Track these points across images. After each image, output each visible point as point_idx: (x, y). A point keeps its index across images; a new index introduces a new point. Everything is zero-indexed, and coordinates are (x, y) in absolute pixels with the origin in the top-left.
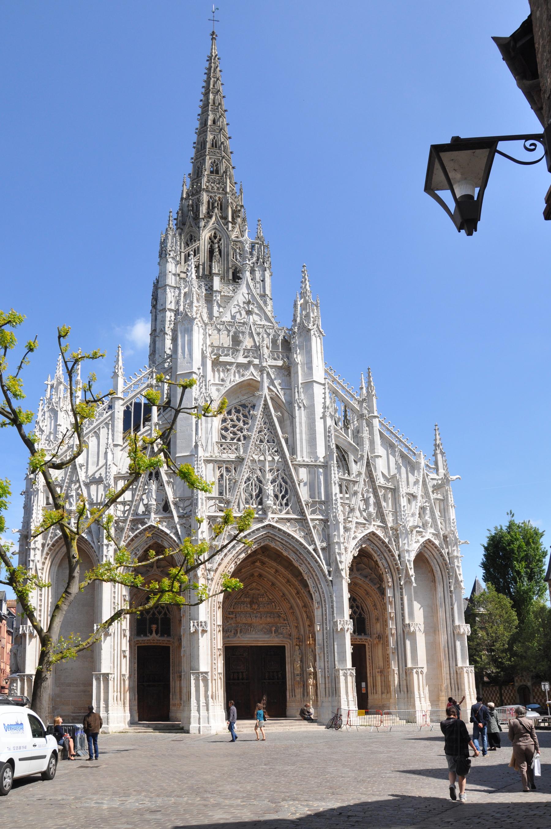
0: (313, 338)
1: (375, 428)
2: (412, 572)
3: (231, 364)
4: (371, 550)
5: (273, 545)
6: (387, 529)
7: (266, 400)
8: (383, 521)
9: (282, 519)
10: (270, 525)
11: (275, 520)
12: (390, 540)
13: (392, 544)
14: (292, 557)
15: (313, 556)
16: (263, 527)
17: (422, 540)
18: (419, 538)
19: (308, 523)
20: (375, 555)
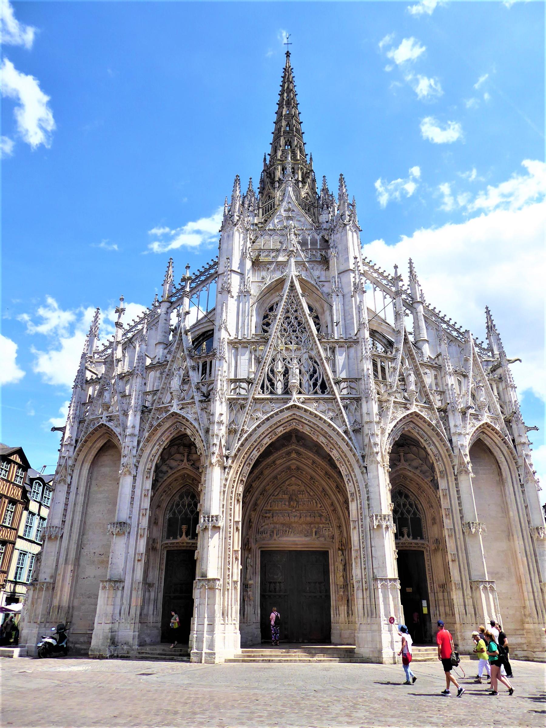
0: (350, 233)
1: (419, 314)
2: (468, 459)
3: (271, 263)
4: (416, 434)
5: (300, 428)
6: (433, 410)
7: (292, 282)
8: (428, 402)
9: (309, 399)
10: (295, 406)
11: (301, 400)
12: (438, 422)
13: (440, 427)
14: (321, 440)
15: (343, 439)
16: (288, 409)
17: (478, 424)
18: (474, 421)
19: (337, 402)
20: (422, 441)
